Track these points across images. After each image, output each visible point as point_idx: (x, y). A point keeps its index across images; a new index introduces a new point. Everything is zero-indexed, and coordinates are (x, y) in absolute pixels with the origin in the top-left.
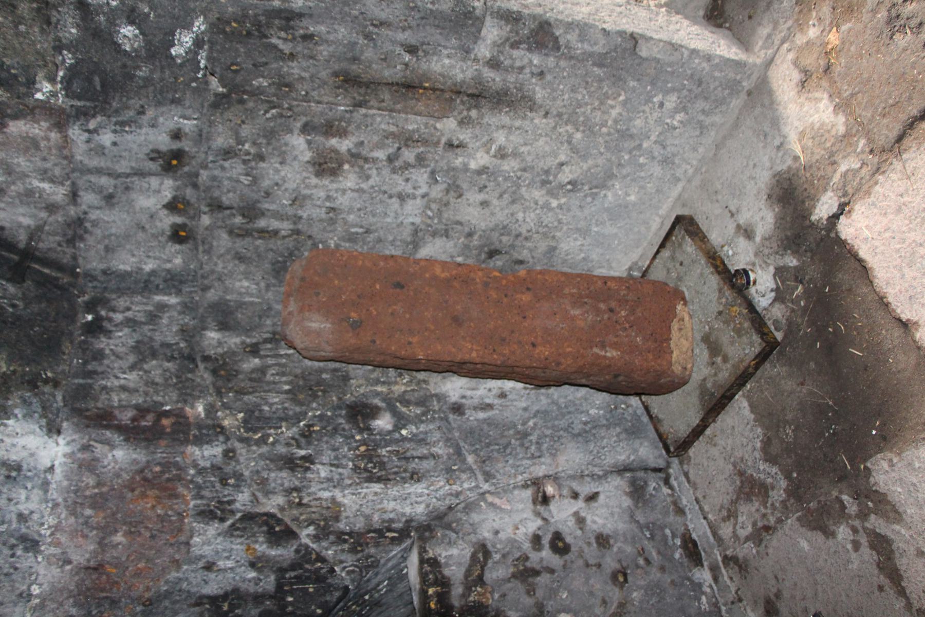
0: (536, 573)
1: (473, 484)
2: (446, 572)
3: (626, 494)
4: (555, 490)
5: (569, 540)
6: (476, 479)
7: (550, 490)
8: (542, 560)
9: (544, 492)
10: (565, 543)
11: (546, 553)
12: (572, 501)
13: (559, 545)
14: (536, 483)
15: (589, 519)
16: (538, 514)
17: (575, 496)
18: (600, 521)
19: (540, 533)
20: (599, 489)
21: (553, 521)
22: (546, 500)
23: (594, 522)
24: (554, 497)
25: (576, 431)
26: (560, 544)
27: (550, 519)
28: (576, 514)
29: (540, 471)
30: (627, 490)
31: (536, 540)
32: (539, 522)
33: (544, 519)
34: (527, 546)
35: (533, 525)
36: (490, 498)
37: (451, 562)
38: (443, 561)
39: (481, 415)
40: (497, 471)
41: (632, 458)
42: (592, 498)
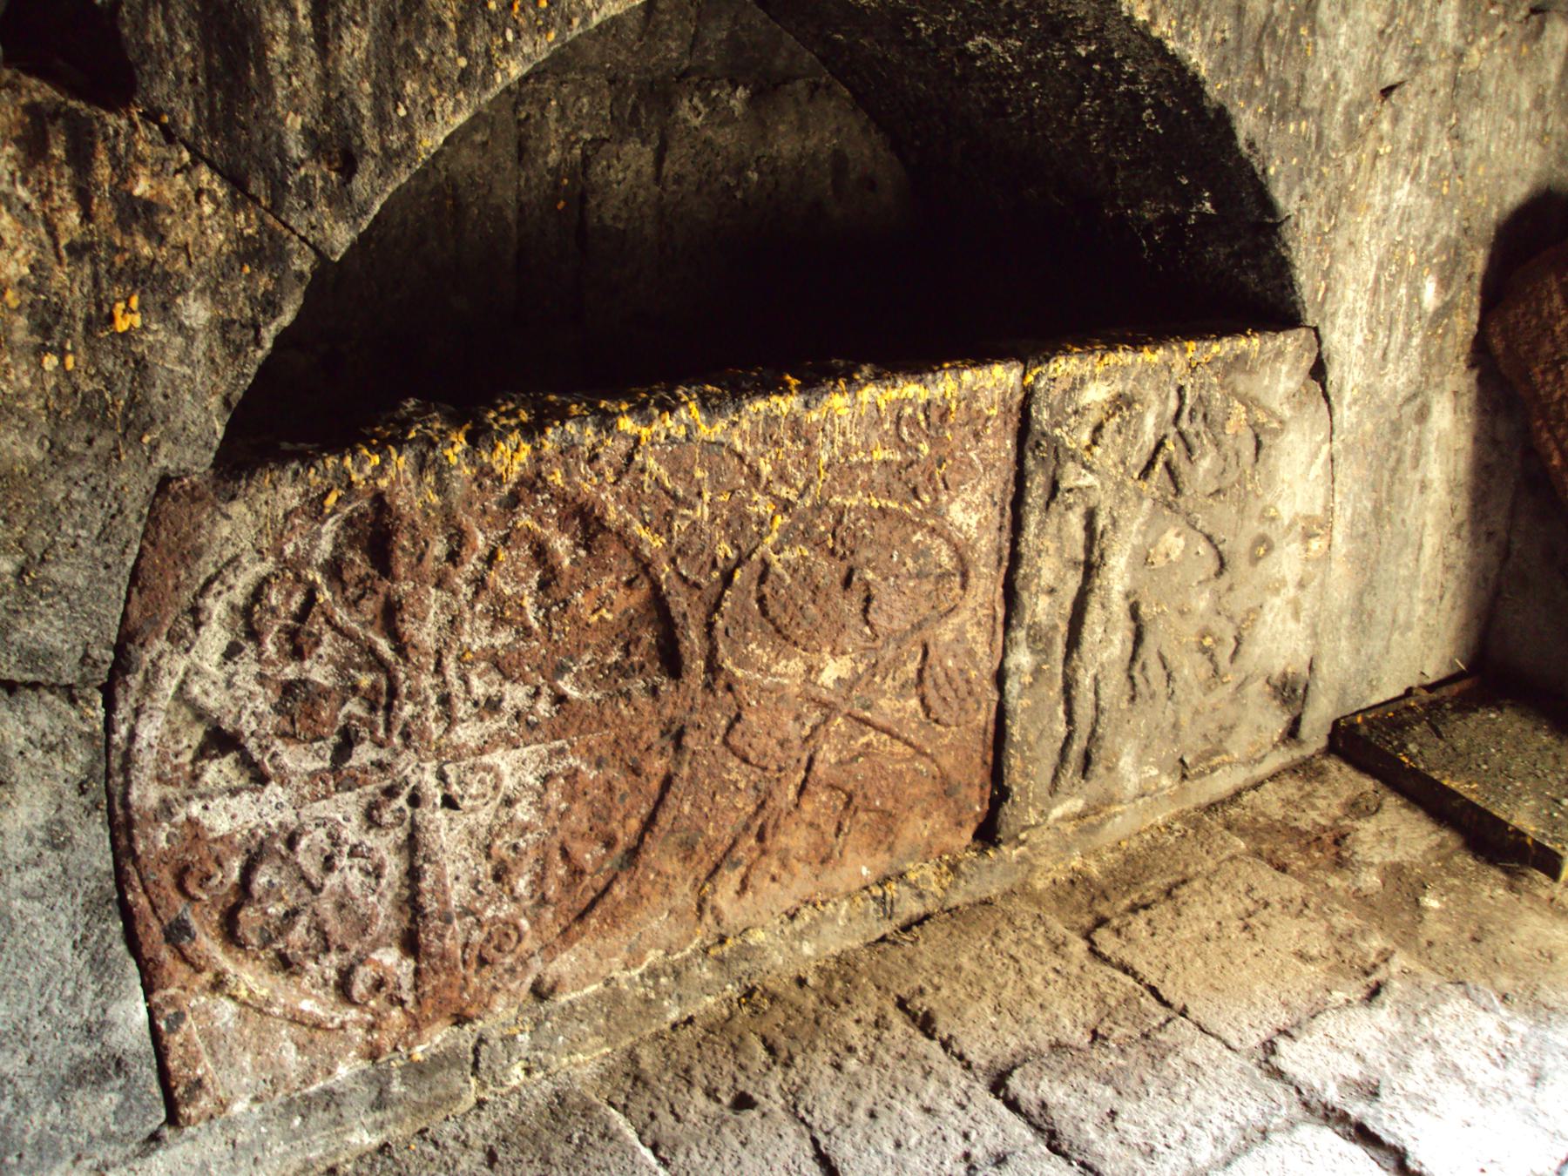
7: (1315, 544)
14: (1326, 525)
17: (1301, 585)
22: (1308, 536)
24: (1307, 550)
25: (1366, 599)
30: (1290, 670)
39: (1409, 450)
41: (1320, 684)
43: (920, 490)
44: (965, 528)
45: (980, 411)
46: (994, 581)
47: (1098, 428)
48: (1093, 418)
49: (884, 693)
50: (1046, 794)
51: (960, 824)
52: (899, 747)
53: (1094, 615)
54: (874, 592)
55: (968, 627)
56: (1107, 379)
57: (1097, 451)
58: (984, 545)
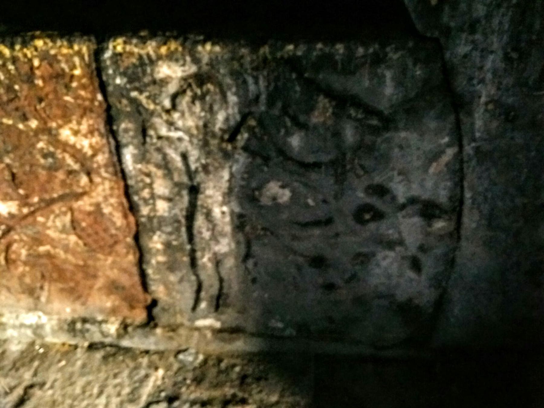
0: (340, 178)
1: (478, 135)
2: (365, 72)
3: (410, 300)
4: (439, 229)
5: (372, 226)
6: (485, 140)
7: (439, 225)
8: (354, 190)
9: (440, 217)
10: (368, 221)
11: (361, 196)
12: (418, 244)
13: (365, 214)
15: (392, 254)
16: (413, 201)
18: (384, 264)
19: (388, 197)
20: (423, 277)
21: (400, 215)
23: (384, 258)
26: (367, 217)
27: (404, 212)
28: (401, 243)
29: (470, 221)
31: (381, 191)
32: (401, 200)
33: (403, 207)
34: (377, 179)
35: (401, 191)
36: (450, 152)
37: (375, 81)
38: (379, 71)
40: (487, 169)
42: (416, 265)
43: (28, 115)
44: (78, 146)
45: (63, 70)
46: (116, 182)
47: (174, 97)
48: (172, 88)
49: (49, 228)
50: (189, 311)
51: (132, 307)
52: (70, 257)
53: (200, 221)
54: (15, 171)
55: (103, 206)
56: (177, 60)
57: (176, 115)
58: (101, 159)
